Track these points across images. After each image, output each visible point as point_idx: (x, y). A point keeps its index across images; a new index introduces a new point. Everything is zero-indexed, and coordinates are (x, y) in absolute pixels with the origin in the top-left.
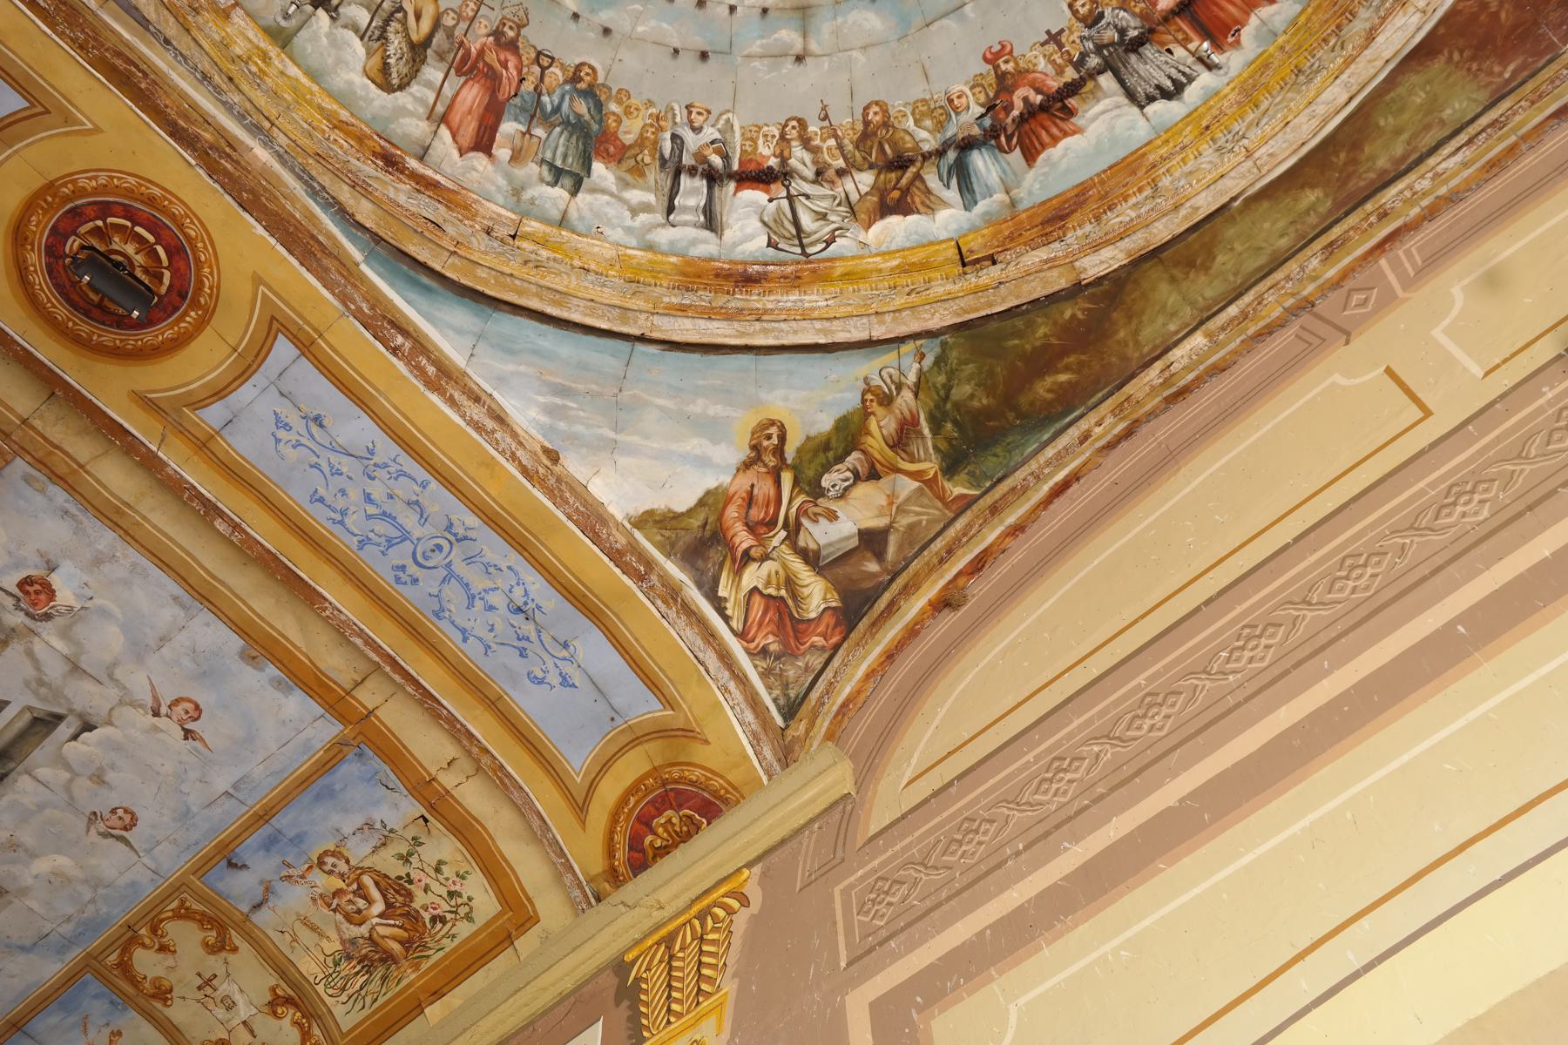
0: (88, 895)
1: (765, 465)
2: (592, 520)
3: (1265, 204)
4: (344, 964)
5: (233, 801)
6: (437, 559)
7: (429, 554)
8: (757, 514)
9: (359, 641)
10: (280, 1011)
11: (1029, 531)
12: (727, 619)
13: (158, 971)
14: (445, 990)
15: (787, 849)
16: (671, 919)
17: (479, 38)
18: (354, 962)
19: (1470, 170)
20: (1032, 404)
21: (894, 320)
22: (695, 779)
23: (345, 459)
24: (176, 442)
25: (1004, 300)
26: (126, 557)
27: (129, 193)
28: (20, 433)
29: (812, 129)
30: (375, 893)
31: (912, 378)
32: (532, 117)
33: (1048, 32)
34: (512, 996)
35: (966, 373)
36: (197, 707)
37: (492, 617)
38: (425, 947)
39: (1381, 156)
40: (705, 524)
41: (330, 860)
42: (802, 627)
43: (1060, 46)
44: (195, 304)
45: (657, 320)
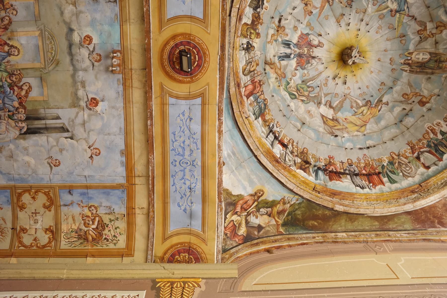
0: (30, 173)
1: (254, 198)
2: (220, 183)
3: (369, 219)
4: (74, 233)
5: (85, 179)
6: (184, 165)
7: (184, 163)
8: (245, 206)
9: (150, 168)
10: (48, 232)
11: (291, 248)
12: (225, 222)
13: (27, 202)
14: (96, 256)
15: (214, 280)
16: (174, 278)
17: (257, 79)
18: (77, 234)
20: (307, 224)
21: (299, 190)
22: (199, 251)
23: (188, 131)
24: (159, 100)
25: (319, 202)
26: (120, 111)
27: (202, 49)
28: (128, 71)
29: (294, 144)
30: (96, 223)
31: (292, 203)
32: (256, 100)
34: (118, 270)
35: (302, 209)
36: (99, 154)
37: (183, 186)
38: (98, 243)
39: (391, 225)
40: (235, 200)
41: (93, 208)
42: (236, 235)
43: (343, 165)
44: (191, 78)
45: (261, 155)
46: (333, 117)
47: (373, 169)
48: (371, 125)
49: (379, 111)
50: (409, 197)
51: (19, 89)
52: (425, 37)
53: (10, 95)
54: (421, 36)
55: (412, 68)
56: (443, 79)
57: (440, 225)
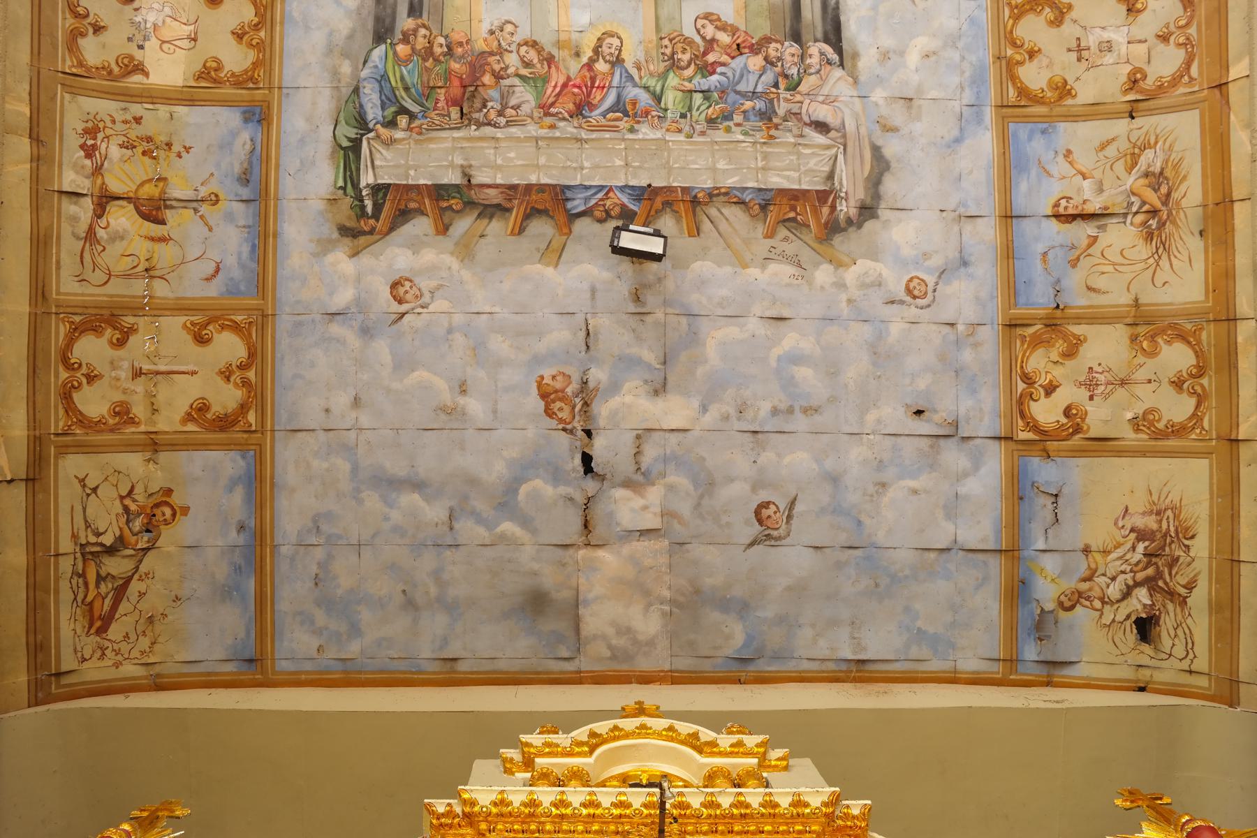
0: (956, 56)
51: (712, 50)
53: (730, 74)
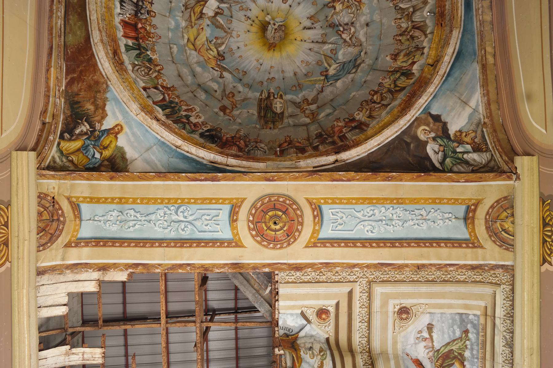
19: (54, 24)
33: (154, 4)
39: (73, 18)
46: (205, 14)
47: (143, 37)
48: (195, 56)
49: (212, 68)
50: (109, 46)
52: (300, 106)
54: (302, 103)
55: (264, 101)
56: (254, 125)
57: (69, 81)
